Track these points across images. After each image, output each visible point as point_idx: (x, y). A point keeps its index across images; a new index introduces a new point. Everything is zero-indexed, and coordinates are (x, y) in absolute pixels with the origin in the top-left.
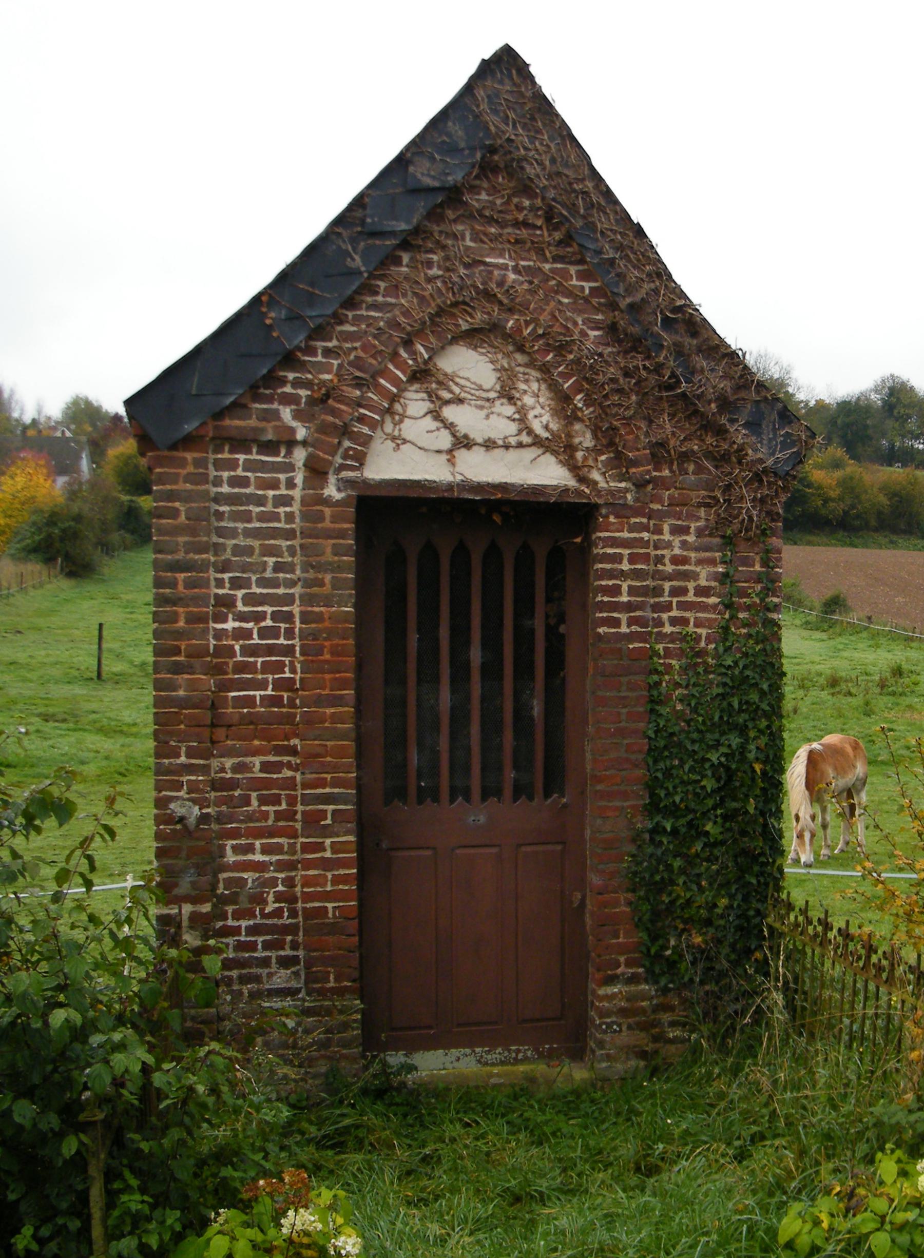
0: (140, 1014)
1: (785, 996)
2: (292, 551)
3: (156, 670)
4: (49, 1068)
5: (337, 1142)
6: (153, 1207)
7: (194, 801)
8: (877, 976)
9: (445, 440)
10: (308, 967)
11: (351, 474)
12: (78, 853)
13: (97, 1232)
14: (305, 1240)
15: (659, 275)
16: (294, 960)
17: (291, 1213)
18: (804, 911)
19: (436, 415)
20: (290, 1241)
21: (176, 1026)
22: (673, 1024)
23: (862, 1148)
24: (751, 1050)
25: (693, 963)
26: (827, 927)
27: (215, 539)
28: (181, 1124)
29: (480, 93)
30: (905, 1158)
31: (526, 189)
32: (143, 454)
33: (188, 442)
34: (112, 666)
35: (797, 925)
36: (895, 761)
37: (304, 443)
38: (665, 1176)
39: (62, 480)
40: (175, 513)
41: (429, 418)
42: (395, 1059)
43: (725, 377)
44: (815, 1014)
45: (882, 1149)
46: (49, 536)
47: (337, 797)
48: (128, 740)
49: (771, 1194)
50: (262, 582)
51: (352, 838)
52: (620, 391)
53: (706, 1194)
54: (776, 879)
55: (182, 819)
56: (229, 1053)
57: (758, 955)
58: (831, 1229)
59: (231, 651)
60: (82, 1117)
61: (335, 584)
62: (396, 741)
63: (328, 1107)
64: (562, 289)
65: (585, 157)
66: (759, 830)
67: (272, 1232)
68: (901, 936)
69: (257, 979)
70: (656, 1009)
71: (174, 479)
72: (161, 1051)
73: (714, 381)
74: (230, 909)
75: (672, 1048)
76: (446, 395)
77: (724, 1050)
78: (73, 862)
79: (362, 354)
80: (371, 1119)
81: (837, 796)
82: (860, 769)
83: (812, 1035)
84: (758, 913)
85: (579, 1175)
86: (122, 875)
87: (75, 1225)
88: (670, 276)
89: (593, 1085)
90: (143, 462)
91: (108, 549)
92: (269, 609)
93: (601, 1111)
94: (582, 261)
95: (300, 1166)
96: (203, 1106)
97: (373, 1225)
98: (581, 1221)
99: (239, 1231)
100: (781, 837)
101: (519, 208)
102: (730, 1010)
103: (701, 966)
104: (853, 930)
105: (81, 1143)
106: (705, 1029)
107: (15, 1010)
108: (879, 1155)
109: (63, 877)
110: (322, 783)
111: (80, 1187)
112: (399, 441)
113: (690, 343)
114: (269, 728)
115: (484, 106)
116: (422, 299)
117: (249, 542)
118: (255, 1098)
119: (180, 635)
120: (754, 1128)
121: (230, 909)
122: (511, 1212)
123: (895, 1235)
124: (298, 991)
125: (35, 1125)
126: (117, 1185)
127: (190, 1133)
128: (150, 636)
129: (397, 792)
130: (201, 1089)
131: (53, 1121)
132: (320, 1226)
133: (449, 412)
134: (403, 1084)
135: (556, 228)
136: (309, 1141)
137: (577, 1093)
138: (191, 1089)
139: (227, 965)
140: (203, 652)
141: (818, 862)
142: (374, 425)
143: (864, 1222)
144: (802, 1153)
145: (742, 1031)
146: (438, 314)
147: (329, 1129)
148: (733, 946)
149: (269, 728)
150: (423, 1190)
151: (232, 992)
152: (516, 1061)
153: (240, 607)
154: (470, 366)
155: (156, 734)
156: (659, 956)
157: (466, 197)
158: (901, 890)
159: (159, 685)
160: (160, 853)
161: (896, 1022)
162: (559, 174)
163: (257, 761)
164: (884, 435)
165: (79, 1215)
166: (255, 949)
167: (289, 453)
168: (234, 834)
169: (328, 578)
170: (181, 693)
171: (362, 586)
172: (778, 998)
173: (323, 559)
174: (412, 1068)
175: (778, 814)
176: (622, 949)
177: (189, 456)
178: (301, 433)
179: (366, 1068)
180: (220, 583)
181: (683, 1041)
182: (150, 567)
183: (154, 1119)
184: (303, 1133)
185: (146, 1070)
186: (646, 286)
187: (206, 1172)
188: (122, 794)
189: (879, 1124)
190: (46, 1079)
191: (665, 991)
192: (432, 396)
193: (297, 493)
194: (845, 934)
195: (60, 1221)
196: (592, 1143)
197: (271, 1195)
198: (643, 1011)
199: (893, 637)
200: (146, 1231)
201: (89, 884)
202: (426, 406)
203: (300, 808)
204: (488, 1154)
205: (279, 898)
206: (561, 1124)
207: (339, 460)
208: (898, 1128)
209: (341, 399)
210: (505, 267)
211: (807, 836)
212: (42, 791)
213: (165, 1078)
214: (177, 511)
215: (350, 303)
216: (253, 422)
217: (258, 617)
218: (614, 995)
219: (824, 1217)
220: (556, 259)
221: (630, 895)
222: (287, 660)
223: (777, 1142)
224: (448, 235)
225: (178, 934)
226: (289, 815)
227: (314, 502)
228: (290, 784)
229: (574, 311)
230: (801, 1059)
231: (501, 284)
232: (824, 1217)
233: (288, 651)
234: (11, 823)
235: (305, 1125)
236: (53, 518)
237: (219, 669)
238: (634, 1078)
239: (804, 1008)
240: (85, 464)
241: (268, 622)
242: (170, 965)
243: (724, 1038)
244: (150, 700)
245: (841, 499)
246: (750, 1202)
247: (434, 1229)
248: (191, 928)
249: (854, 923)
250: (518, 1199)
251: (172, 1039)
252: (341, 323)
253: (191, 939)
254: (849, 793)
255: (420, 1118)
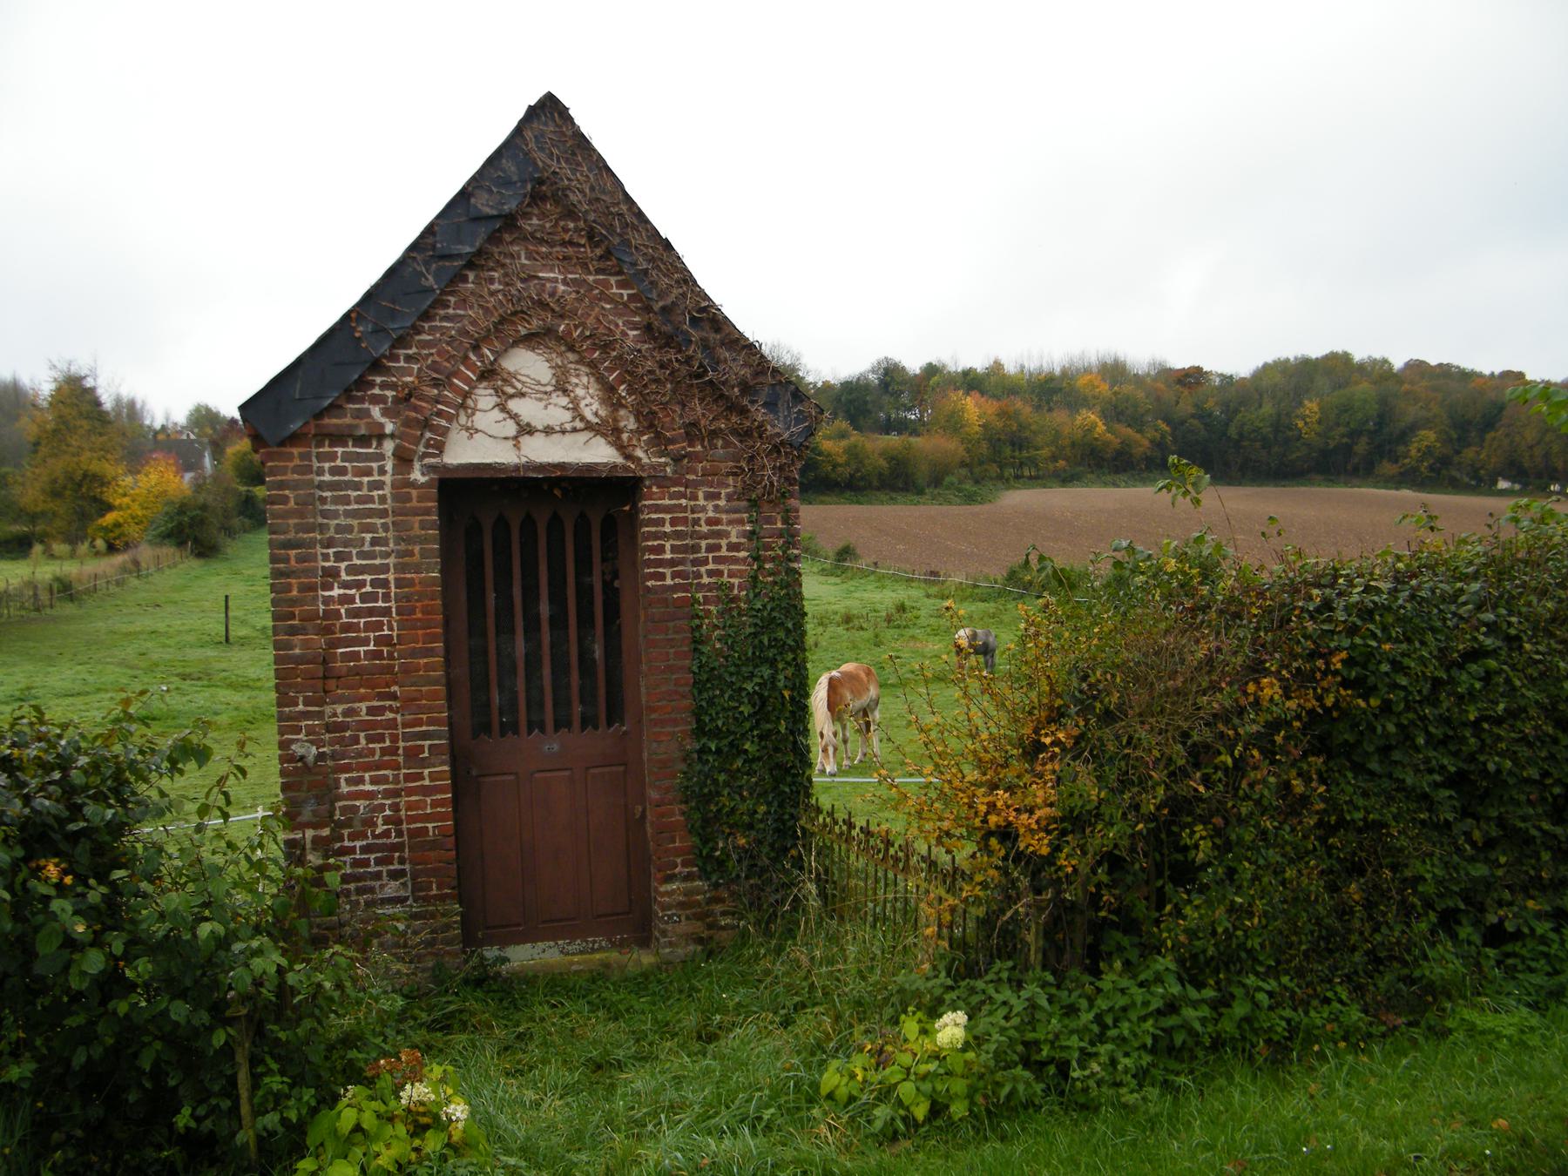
0: (274, 924)
1: (818, 886)
2: (385, 527)
3: (275, 634)
4: (199, 973)
5: (445, 1025)
6: (292, 1086)
7: (312, 742)
8: (895, 866)
9: (511, 428)
10: (413, 879)
11: (432, 460)
12: (216, 790)
13: (245, 1109)
14: (421, 1109)
15: (686, 282)
16: (402, 873)
17: (408, 1087)
18: (831, 814)
19: (502, 408)
20: (409, 1110)
21: (304, 932)
22: (724, 914)
23: (888, 1012)
24: (790, 933)
25: (739, 861)
26: (851, 826)
27: (320, 520)
28: (312, 1015)
29: (528, 134)
30: (924, 1018)
31: (571, 213)
32: (256, 451)
33: (294, 439)
34: (237, 631)
35: (825, 825)
36: (902, 683)
37: (392, 436)
38: (722, 1043)
39: (188, 476)
40: (285, 500)
41: (496, 410)
42: (491, 953)
43: (745, 365)
44: (843, 900)
45: (905, 1012)
46: (180, 523)
47: (432, 734)
48: (254, 693)
49: (813, 1054)
50: (361, 555)
51: (446, 768)
52: (657, 381)
53: (758, 1056)
54: (805, 788)
55: (302, 758)
56: (350, 953)
57: (794, 852)
58: (865, 1081)
59: (337, 614)
60: (228, 1013)
61: (423, 554)
62: (480, 685)
63: (435, 996)
64: (604, 297)
65: (619, 184)
66: (790, 746)
67: (393, 1103)
68: (914, 831)
69: (371, 890)
70: (710, 901)
71: (284, 471)
72: (293, 954)
73: (736, 369)
74: (346, 832)
75: (724, 934)
76: (510, 390)
77: (768, 934)
78: (212, 798)
79: (437, 359)
80: (472, 1004)
81: (854, 715)
82: (873, 692)
83: (842, 918)
84: (792, 816)
85: (651, 1044)
86: (254, 807)
87: (226, 1104)
88: (695, 282)
89: (659, 968)
90: (257, 457)
91: (230, 532)
92: (368, 578)
93: (666, 990)
94: (620, 273)
95: (415, 1047)
96: (331, 1000)
97: (478, 1094)
98: (653, 1083)
99: (365, 1104)
100: (809, 751)
101: (566, 230)
102: (772, 900)
103: (745, 863)
104: (873, 828)
105: (229, 1035)
106: (751, 916)
107: (168, 925)
108: (903, 1017)
109: (204, 811)
110: (419, 723)
111: (229, 1072)
112: (472, 431)
113: (714, 337)
114: (372, 678)
115: (532, 145)
116: (486, 310)
117: (349, 521)
118: (373, 991)
119: (294, 602)
120: (797, 999)
121: (346, 832)
122: (594, 1078)
123: (919, 1084)
124: (406, 899)
125: (189, 1022)
126: (260, 1069)
127: (320, 1022)
128: (269, 604)
129: (484, 728)
130: (327, 985)
131: (204, 1017)
132: (433, 1097)
133: (513, 405)
134: (498, 974)
135: (597, 245)
136: (421, 1025)
137: (645, 975)
138: (319, 986)
139: (346, 879)
140: (311, 617)
141: (841, 772)
142: (450, 418)
143: (892, 1074)
144: (838, 1018)
145: (783, 917)
146: (500, 323)
147: (437, 1014)
148: (772, 846)
149: (372, 678)
150: (519, 1062)
151: (350, 902)
152: (593, 951)
153: (344, 577)
154: (530, 365)
155: (277, 686)
156: (709, 856)
157: (520, 223)
158: (912, 792)
159: (278, 646)
160: (285, 788)
161: (913, 904)
162: (598, 200)
163: (363, 706)
164: (881, 409)
165: (229, 1096)
166: (368, 865)
167: (380, 445)
168: (347, 768)
169: (417, 549)
170: (297, 651)
171: (446, 554)
172: (812, 887)
173: (412, 533)
174: (505, 960)
175: (806, 732)
176: (679, 852)
177: (296, 451)
178: (389, 428)
179: (466, 961)
180: (326, 557)
181: (733, 927)
182: (266, 546)
183: (289, 1012)
184: (415, 1019)
185: (281, 971)
186: (676, 292)
187: (335, 1056)
188: (250, 739)
189: (901, 991)
190: (196, 982)
191: (716, 886)
192: (498, 392)
193: (388, 479)
194: (866, 832)
195: (213, 1101)
196: (660, 1017)
197: (390, 1072)
198: (699, 904)
199: (896, 579)
200: (286, 1107)
201: (226, 816)
202: (495, 400)
203: (401, 744)
204: (573, 1030)
205: (387, 820)
206: (634, 1003)
207: (422, 449)
208: (918, 994)
209: (422, 398)
210: (555, 280)
211: (831, 750)
212: (183, 739)
213: (297, 977)
214: (287, 497)
215: (426, 316)
216: (348, 420)
217: (361, 584)
218: (673, 891)
219: (858, 1071)
220: (598, 271)
221: (683, 807)
222: (385, 620)
223: (816, 1010)
224: (506, 255)
225: (303, 854)
226: (393, 751)
227: (402, 486)
228: (392, 724)
229: (615, 315)
230: (833, 939)
231: (552, 295)
232: (858, 1071)
233: (386, 612)
234: (158, 767)
235: (417, 1012)
236: (182, 509)
237: (328, 630)
238: (693, 961)
239: (834, 896)
240: (207, 461)
241: (368, 589)
242: (298, 882)
243: (767, 924)
244: (271, 658)
245: (847, 464)
246: (796, 1061)
247: (530, 1095)
248: (314, 849)
249: (874, 822)
250: (599, 1067)
251: (301, 944)
252: (419, 333)
253: (314, 859)
254: (865, 712)
255: (514, 1002)
